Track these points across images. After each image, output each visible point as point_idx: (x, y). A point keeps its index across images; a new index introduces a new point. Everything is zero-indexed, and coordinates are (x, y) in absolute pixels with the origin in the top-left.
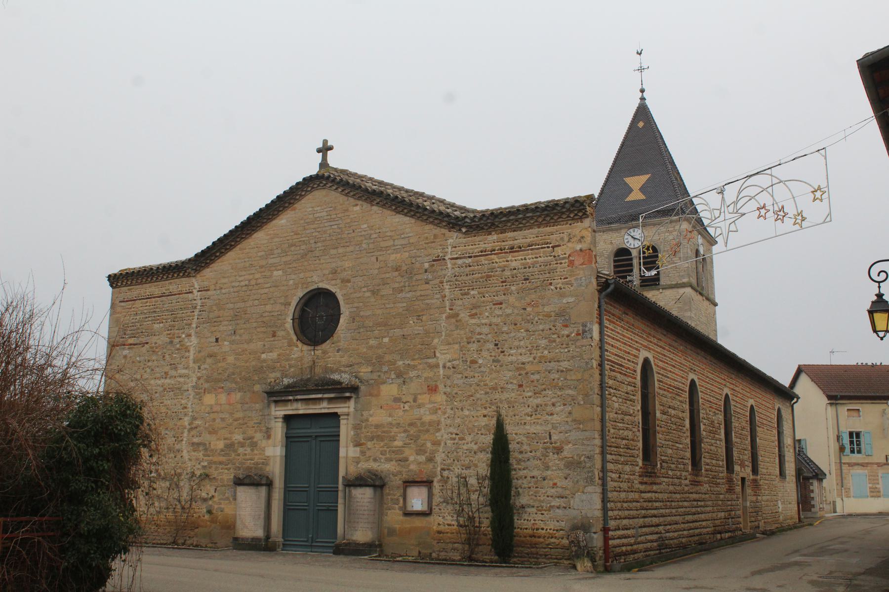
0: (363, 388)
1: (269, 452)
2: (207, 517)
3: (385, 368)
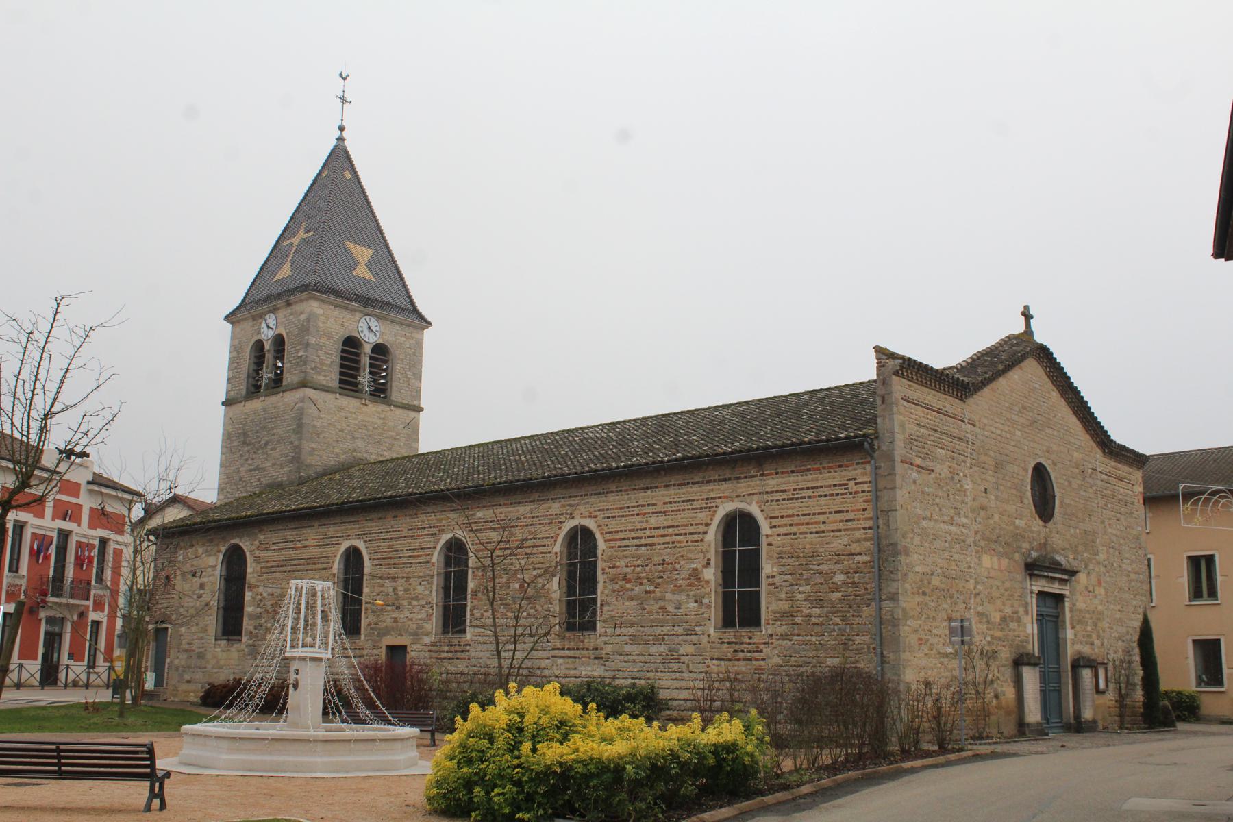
2: (995, 702)
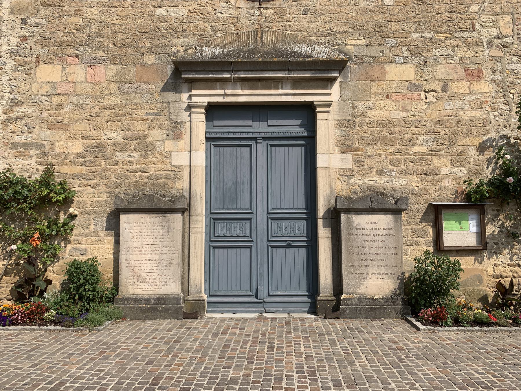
0: (352, 67)
1: (180, 159)
3: (391, 42)
